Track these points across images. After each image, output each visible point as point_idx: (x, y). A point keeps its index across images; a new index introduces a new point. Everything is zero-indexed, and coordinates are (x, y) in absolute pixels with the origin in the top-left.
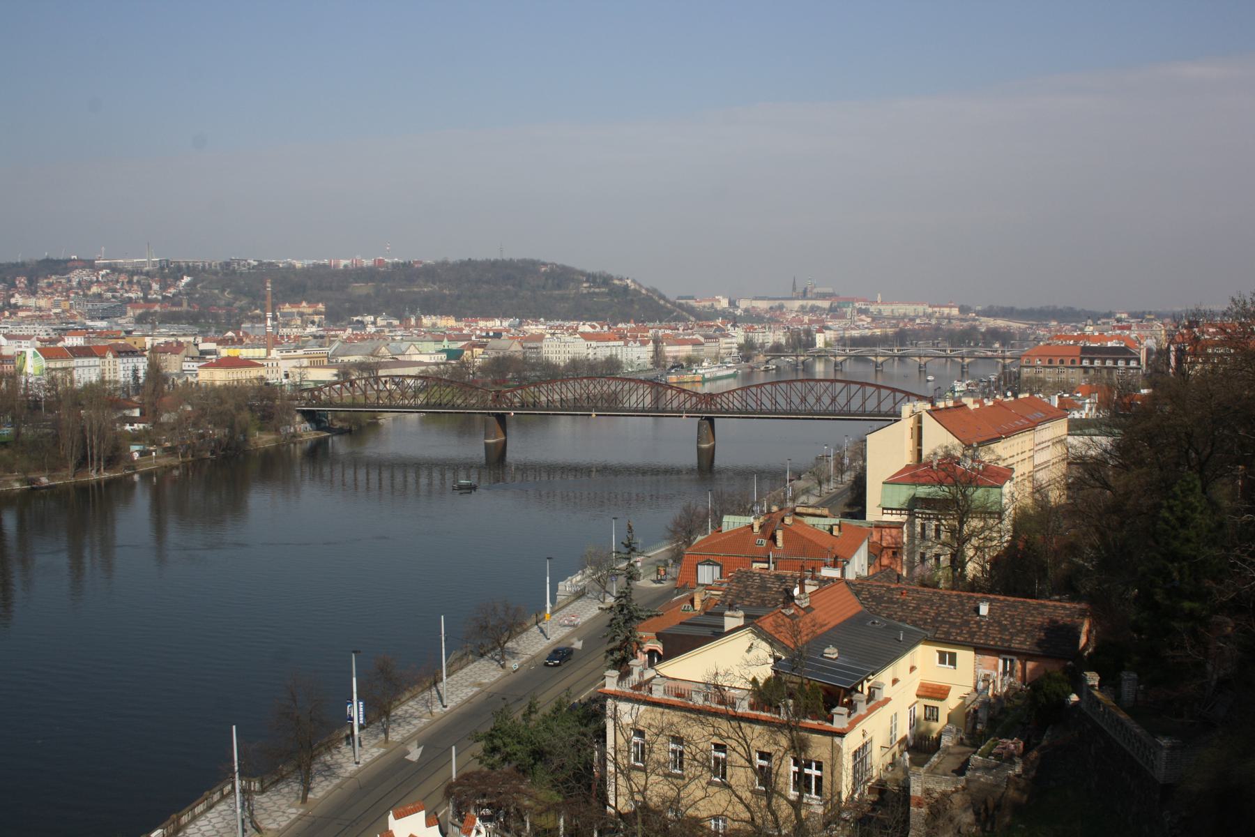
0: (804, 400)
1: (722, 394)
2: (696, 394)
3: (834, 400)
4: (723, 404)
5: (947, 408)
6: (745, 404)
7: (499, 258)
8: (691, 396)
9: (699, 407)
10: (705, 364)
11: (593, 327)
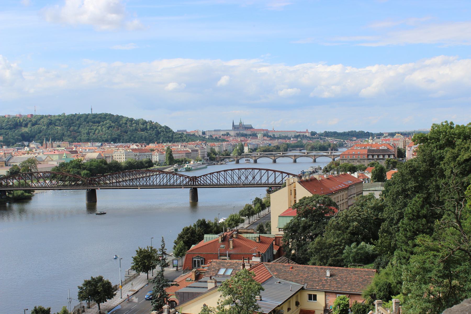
0: (239, 178)
1: (201, 177)
2: (188, 177)
3: (254, 178)
5: (307, 181)
8: (186, 178)
9: (190, 183)
10: (192, 162)
11: (137, 146)
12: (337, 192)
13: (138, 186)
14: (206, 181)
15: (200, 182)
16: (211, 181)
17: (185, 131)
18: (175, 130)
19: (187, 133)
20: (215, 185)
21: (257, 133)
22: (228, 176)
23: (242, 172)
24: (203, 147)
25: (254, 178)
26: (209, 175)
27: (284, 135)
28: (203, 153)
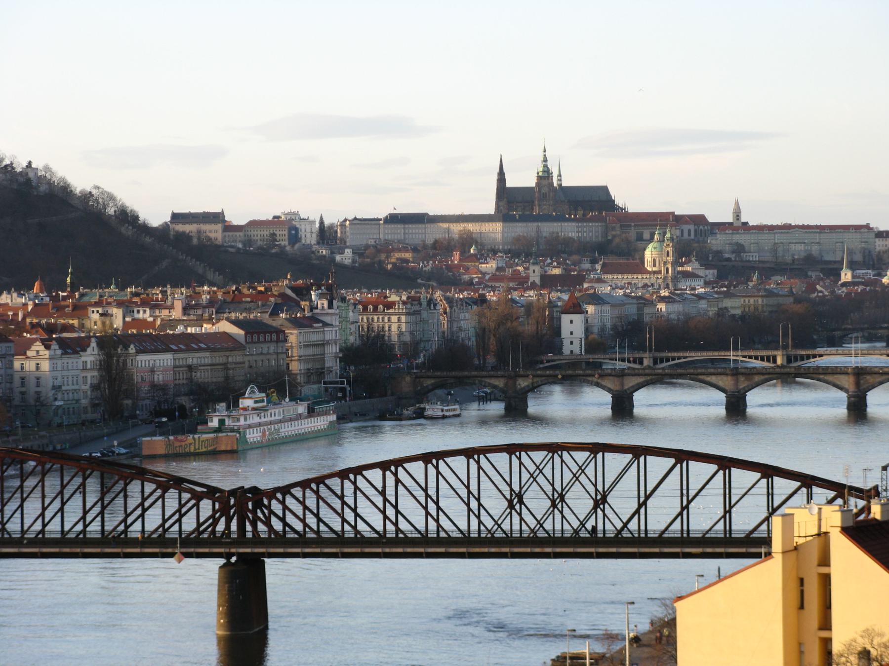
0: (516, 500)
1: (286, 490)
2: (212, 492)
3: (600, 501)
4: (290, 518)
6: (349, 515)
8: (198, 497)
9: (221, 527)
14: (317, 516)
15: (283, 520)
16: (344, 520)
17: (217, 218)
19: (229, 228)
20: (370, 542)
21: (640, 238)
22: (362, 503)
23: (532, 468)
24: (314, 319)
25: (604, 500)
26: (335, 483)
27: (798, 250)
28: (317, 351)
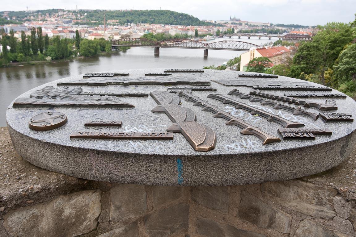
0: (229, 45)
2: (204, 44)
3: (236, 46)
5: (261, 49)
7: (160, 10)
11: (182, 27)
12: (273, 56)
13: (179, 47)
18: (201, 20)
